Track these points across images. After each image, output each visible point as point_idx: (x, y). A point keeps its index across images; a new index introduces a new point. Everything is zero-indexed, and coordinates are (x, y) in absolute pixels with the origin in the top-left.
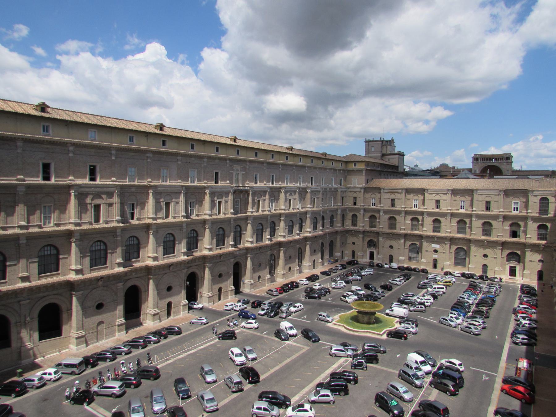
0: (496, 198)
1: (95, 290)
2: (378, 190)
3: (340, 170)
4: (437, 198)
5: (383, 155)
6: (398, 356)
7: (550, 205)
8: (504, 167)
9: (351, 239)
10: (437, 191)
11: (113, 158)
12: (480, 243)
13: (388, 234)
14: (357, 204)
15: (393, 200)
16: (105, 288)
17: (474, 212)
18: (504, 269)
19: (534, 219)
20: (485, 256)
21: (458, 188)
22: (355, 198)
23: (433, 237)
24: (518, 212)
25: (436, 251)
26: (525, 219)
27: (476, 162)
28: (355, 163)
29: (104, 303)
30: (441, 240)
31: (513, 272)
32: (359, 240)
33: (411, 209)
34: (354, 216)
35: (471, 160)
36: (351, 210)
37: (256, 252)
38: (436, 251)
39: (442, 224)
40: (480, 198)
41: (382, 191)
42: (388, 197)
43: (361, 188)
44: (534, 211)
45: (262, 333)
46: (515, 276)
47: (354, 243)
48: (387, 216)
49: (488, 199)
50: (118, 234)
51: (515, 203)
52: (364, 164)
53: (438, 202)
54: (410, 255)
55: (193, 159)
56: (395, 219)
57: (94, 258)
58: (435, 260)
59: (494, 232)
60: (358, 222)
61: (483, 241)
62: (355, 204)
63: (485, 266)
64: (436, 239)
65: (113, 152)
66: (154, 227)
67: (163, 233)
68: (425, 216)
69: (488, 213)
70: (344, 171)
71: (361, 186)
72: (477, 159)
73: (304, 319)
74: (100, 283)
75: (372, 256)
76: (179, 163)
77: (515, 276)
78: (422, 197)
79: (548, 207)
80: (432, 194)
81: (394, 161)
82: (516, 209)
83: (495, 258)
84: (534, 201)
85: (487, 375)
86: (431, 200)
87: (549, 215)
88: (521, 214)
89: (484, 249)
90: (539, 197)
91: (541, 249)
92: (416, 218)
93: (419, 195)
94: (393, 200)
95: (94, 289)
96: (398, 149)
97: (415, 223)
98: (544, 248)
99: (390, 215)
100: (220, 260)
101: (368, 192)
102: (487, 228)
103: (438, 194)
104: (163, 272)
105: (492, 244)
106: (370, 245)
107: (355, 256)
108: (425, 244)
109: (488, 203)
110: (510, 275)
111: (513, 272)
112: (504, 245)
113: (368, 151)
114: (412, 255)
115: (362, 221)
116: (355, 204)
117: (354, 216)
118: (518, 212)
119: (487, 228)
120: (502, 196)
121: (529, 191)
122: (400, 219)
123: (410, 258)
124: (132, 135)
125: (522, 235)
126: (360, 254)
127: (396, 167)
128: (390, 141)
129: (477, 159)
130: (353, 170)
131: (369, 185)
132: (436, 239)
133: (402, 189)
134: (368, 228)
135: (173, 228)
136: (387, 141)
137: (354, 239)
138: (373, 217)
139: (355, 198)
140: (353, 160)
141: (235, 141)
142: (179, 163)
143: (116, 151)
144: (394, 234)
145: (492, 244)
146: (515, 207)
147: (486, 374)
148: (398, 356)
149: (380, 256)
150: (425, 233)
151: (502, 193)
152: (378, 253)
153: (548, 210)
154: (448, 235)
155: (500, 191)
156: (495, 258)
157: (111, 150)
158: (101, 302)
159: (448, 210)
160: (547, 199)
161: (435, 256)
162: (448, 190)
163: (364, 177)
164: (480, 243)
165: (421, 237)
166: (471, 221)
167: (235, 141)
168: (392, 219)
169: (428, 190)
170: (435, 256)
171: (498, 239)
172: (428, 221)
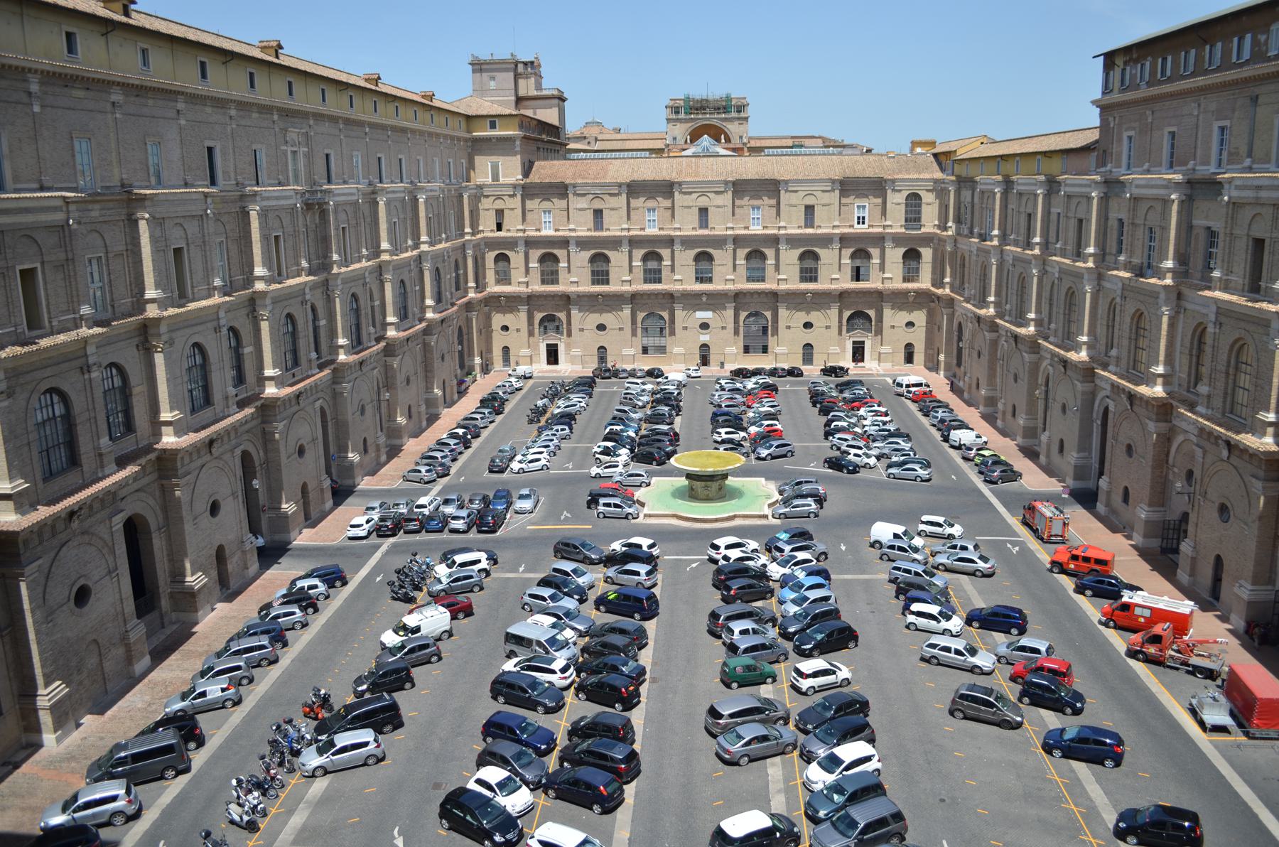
0: (826, 198)
1: (64, 549)
2: (561, 190)
3: (459, 139)
4: (703, 202)
5: (519, 100)
6: (843, 548)
7: (924, 208)
8: (733, 128)
9: (498, 320)
10: (703, 187)
11: (37, 109)
12: (797, 300)
13: (593, 297)
14: (505, 227)
15: (598, 213)
16: (86, 538)
17: (782, 232)
18: (843, 350)
19: (898, 240)
20: (808, 325)
21: (745, 177)
22: (500, 213)
23: (698, 295)
24: (866, 226)
25: (705, 326)
26: (879, 240)
27: (674, 116)
28: (492, 120)
29: (90, 584)
30: (715, 301)
31: (858, 353)
32: (518, 320)
33: (642, 233)
34: (502, 258)
35: (665, 114)
36: (491, 244)
37: (354, 376)
38: (705, 326)
39: (716, 262)
40: (794, 199)
41: (570, 192)
42: (585, 206)
43: (515, 186)
44: (896, 223)
45: (517, 571)
46: (862, 360)
47: (505, 328)
48: (587, 255)
49: (810, 201)
50: (91, 360)
51: (859, 207)
52: (517, 121)
53: (703, 212)
54: (646, 341)
55: (208, 110)
56: (607, 259)
57: (44, 448)
58: (705, 347)
59: (822, 272)
60: (513, 272)
61: (803, 294)
62: (499, 227)
63: (808, 347)
64: (704, 299)
65: (34, 88)
66: (163, 328)
67: (183, 341)
68: (677, 248)
69: (810, 231)
70: (466, 140)
71: (511, 180)
72: (677, 110)
73: (567, 521)
74: (75, 524)
75: (553, 356)
76: (183, 122)
77: (862, 360)
78: (668, 203)
79: (919, 212)
80: (690, 193)
81: (548, 115)
82: (861, 220)
83: (827, 327)
84: (896, 200)
85: (1014, 544)
86: (690, 207)
87: (923, 230)
88: (871, 230)
89: (808, 313)
90: (906, 193)
91: (911, 299)
92: (652, 252)
93: (659, 199)
94: (598, 213)
95: (63, 545)
96: (550, 85)
97: (652, 265)
98: (915, 297)
99: (593, 252)
100: (296, 408)
101: (532, 197)
102: (809, 267)
103: (703, 194)
104: (199, 463)
105: (821, 300)
106: (545, 328)
107: (513, 359)
108: (680, 314)
109: (810, 210)
110: (854, 361)
111: (858, 353)
112: (842, 296)
113: (480, 91)
114: (649, 341)
115: (523, 269)
116: (499, 227)
117: (502, 258)
118: (866, 226)
119: (809, 267)
120: (837, 192)
121: (886, 181)
122: (618, 259)
123: (645, 350)
124: (70, 30)
125: (874, 273)
126: (525, 352)
127: (554, 130)
128: (532, 63)
129: (677, 110)
130: (488, 140)
131: (534, 178)
132: (704, 299)
133: (620, 185)
134: (538, 287)
135: (199, 328)
136: (525, 64)
137: (508, 319)
138: (549, 259)
139: (500, 213)
140: (484, 113)
141: (277, 57)
142: (183, 122)
143: (42, 83)
144: (605, 296)
145: (821, 300)
146: (861, 217)
147: (1011, 542)
148: (843, 548)
149: (576, 351)
150: (678, 287)
151: (838, 185)
152: (568, 347)
153: (919, 220)
154: (730, 287)
155: (833, 181)
156: (827, 327)
157: (26, 81)
158: (82, 582)
159: (727, 228)
160: (920, 199)
161: (705, 338)
162: (726, 183)
163: (519, 157)
164: (797, 300)
165: (670, 297)
166: (778, 251)
167: (277, 57)
168: (599, 259)
169: (680, 184)
170: (705, 338)
171: (833, 287)
172: (790, 257)
